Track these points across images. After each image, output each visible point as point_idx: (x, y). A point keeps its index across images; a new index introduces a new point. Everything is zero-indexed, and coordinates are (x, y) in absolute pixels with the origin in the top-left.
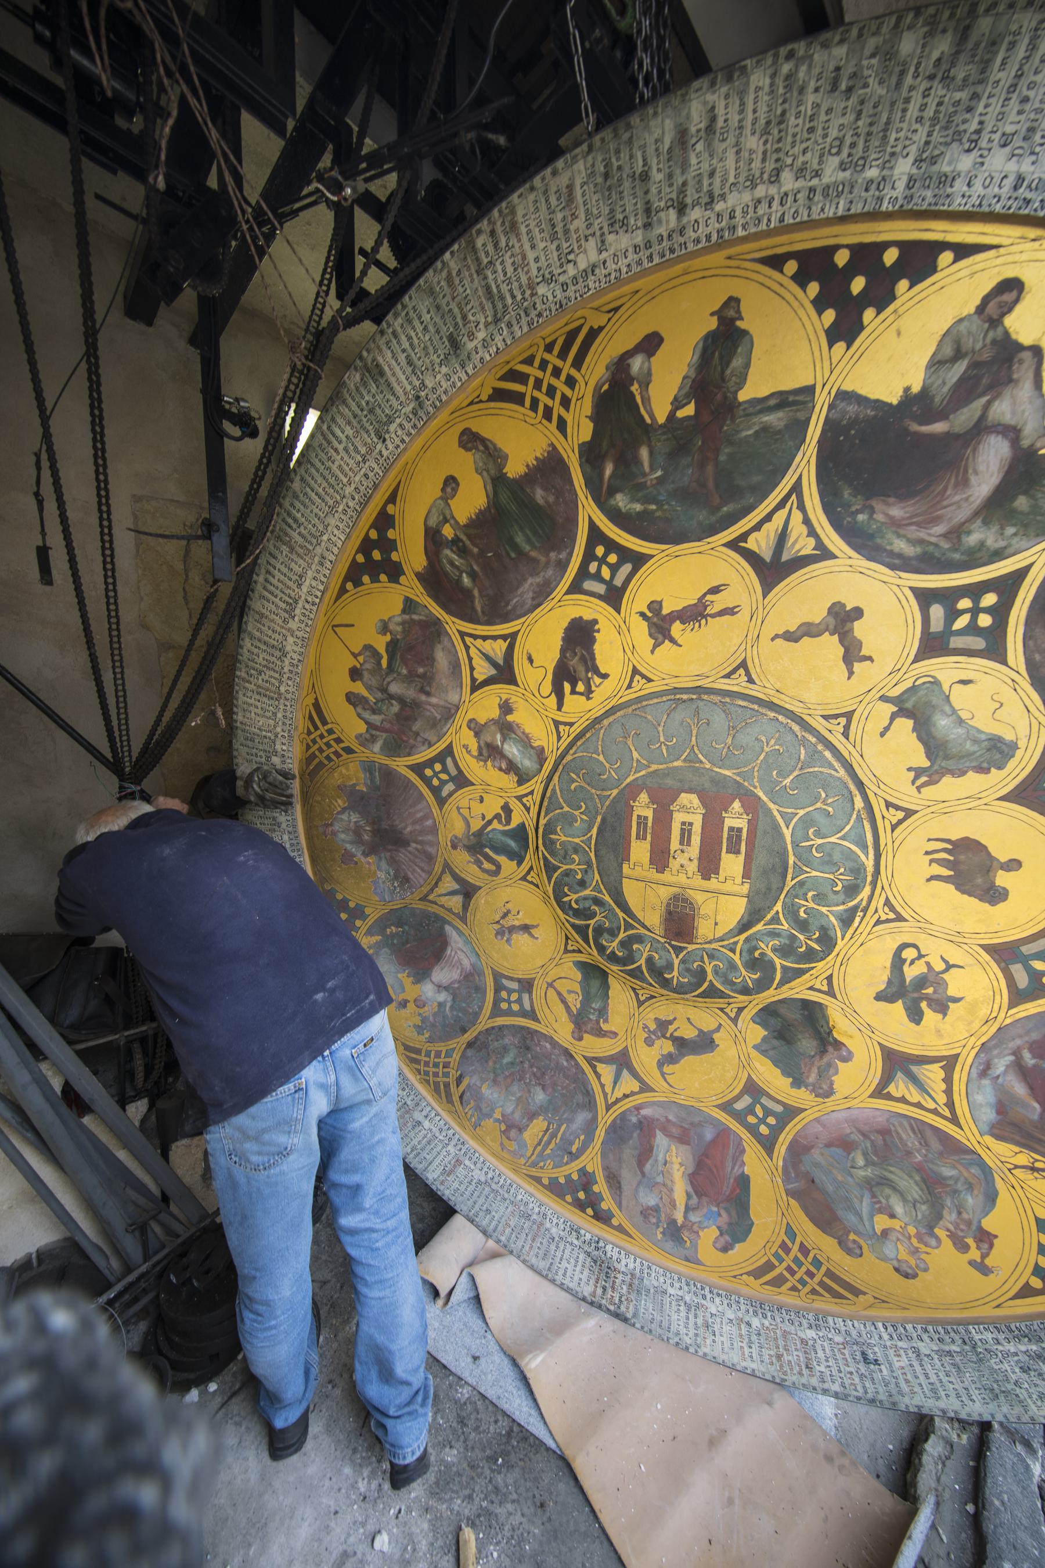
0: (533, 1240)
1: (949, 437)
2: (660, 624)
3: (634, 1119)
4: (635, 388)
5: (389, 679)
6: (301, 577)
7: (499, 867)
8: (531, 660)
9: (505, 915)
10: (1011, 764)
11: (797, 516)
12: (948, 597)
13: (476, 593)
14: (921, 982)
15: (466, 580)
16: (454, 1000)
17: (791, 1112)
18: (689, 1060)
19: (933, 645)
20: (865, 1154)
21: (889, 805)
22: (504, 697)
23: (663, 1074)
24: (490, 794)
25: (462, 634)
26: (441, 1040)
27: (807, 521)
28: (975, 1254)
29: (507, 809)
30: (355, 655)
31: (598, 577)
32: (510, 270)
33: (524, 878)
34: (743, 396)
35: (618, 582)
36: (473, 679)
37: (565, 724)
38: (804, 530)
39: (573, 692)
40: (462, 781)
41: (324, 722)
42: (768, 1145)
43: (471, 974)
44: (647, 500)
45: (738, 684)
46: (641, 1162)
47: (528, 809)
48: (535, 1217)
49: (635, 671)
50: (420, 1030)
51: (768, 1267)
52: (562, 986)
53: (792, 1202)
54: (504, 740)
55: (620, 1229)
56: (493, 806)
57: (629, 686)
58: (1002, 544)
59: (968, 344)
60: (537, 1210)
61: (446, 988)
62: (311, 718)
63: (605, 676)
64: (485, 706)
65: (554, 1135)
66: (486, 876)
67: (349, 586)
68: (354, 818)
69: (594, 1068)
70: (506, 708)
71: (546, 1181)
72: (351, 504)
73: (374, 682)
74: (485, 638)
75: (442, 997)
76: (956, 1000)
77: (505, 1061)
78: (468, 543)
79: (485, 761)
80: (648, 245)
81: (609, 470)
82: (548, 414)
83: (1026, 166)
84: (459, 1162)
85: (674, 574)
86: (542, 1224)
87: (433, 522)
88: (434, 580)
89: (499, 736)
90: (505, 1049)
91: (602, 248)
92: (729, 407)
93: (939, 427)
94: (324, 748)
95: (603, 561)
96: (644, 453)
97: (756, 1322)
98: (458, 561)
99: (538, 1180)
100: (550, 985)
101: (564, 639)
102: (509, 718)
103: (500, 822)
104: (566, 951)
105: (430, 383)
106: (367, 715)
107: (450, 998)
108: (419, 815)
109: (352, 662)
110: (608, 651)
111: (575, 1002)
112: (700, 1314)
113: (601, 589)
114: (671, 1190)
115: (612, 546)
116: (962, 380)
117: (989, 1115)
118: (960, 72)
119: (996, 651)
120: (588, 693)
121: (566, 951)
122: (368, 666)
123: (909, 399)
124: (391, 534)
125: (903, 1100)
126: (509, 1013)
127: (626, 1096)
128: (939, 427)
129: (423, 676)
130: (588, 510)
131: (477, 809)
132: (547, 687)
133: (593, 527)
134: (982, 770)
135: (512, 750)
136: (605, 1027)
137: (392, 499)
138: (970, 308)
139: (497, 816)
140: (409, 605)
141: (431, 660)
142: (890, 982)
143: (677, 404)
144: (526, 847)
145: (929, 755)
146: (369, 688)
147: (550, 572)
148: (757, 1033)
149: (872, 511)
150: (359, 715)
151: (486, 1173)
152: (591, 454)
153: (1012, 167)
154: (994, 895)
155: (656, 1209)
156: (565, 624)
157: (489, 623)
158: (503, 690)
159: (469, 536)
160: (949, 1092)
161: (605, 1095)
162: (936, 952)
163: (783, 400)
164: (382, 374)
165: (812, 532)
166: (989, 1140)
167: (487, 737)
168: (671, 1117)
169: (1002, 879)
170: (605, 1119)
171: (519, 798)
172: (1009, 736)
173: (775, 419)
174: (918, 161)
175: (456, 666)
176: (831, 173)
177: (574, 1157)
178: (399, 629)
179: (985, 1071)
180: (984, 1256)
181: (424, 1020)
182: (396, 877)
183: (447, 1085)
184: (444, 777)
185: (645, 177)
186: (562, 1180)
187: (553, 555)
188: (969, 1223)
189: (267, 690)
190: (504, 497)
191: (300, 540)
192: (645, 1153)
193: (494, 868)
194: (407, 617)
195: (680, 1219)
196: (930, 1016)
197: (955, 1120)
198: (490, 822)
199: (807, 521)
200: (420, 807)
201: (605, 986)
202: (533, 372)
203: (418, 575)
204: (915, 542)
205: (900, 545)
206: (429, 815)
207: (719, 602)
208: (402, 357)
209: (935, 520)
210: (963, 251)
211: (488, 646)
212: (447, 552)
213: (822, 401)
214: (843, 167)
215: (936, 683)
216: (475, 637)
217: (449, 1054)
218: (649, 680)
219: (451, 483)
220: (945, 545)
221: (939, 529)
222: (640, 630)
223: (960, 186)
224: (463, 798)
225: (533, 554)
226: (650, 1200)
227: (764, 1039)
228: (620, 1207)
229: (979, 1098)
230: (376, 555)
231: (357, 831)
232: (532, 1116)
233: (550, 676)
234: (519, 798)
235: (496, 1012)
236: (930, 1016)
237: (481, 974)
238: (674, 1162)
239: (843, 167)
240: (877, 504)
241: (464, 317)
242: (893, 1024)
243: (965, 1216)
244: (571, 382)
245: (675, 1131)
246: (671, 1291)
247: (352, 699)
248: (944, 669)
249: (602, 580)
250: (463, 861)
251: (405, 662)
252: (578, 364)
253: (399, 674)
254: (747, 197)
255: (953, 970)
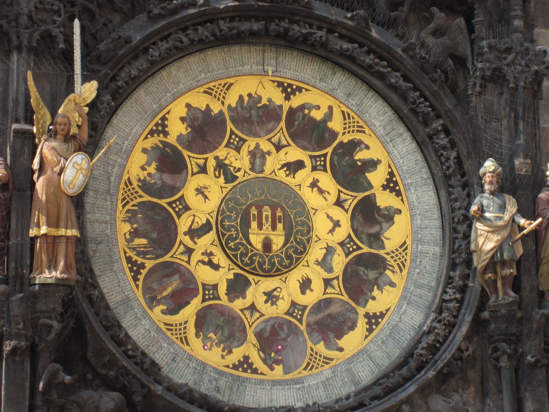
0: (104, 264)
1: (376, 219)
2: (314, 184)
3: (175, 266)
4: (358, 148)
5: (255, 109)
6: (271, 65)
7: (219, 177)
8: (286, 154)
9: (205, 188)
10: (330, 274)
11: (351, 201)
12: (352, 240)
13: (295, 128)
14: (275, 297)
15: (297, 123)
16: (161, 187)
17: (218, 298)
18: (208, 268)
19: (342, 244)
20: (224, 319)
21: (307, 261)
22: (272, 151)
23: (197, 264)
24: (240, 161)
25: (282, 129)
26: (143, 190)
27: (351, 203)
28: (224, 354)
29: (239, 170)
30: (256, 93)
31: (316, 162)
32: (368, 104)
33: (221, 187)
34: (367, 174)
35: (318, 168)
36: (271, 138)
37: (275, 173)
38: (349, 204)
39: (285, 171)
40: (238, 149)
41: (228, 89)
42: (204, 300)
43: (176, 188)
44: (338, 164)
45: (312, 212)
46: (164, 276)
47: (244, 176)
48: (113, 259)
49: (300, 185)
50: (139, 180)
51: (172, 325)
52: (197, 219)
53: (195, 317)
54: (259, 157)
55: (137, 286)
56: (237, 165)
57: (295, 186)
58: (364, 241)
59: (391, 211)
60: (117, 258)
61: (163, 182)
62: (225, 84)
63: (294, 178)
64: (266, 146)
65: (145, 248)
66: (213, 174)
67: (276, 84)
68: (200, 115)
69: (180, 245)
70: (269, 153)
71: (127, 255)
72: (300, 77)
73: (251, 104)
74: (284, 136)
75: (159, 182)
76: (277, 305)
77: (156, 217)
78: (306, 119)
79: (249, 154)
80: (383, 137)
81: (340, 151)
82: (345, 128)
83: (415, 201)
84: (106, 223)
85: (327, 181)
86: (113, 263)
87: (306, 105)
88: (292, 112)
89: (259, 155)
90: (159, 214)
91: (379, 126)
92: (363, 173)
93: (377, 216)
94: (218, 93)
95: (321, 161)
96: (347, 158)
97: (153, 333)
98: (300, 118)
99: (125, 253)
100: (194, 216)
101: (297, 161)
102: (267, 156)
103: (234, 170)
104: (209, 214)
105: (338, 91)
106: (239, 105)
107: (160, 185)
108: (217, 140)
109: (253, 94)
110: (301, 174)
111: (195, 226)
112: (138, 321)
113: (314, 164)
114: (165, 289)
115: (325, 161)
116: (385, 214)
117: (258, 330)
118: (423, 182)
119: (347, 255)
120: (287, 175)
121: (209, 214)
122: (255, 99)
123: (379, 207)
124: (297, 93)
125: (245, 315)
126: (174, 209)
127: (180, 259)
128: (377, 216)
129: (263, 121)
130: (329, 150)
131: (233, 159)
132: (282, 163)
133: (326, 154)
134: (325, 271)
135: (258, 162)
136: (196, 240)
137: (307, 90)
138: (396, 207)
139: (235, 168)
140: (281, 107)
141: (269, 121)
142: (269, 292)
143: (359, 160)
144: (232, 182)
145: (322, 260)
146: (248, 102)
147: (311, 147)
148: (231, 276)
149: (359, 215)
150: (237, 103)
151: (112, 235)
152: (341, 144)
153: (414, 199)
154: (303, 292)
155: (154, 290)
156: (301, 159)
157: (290, 136)
158: (273, 150)
159: (308, 119)
160: (255, 320)
161: (175, 253)
162: (284, 293)
163: (369, 183)
164: (334, 75)
165: (349, 206)
166: (252, 335)
167: (257, 152)
168: (187, 275)
169: (308, 291)
170: (167, 258)
171: (245, 172)
172: (334, 270)
173: (365, 184)
174: (411, 183)
175: (271, 131)
176: (405, 168)
177: (144, 258)
178: (272, 106)
179: (267, 321)
180: (226, 355)
181: (145, 179)
182: (189, 142)
183: (128, 202)
184: (235, 143)
185: (393, 130)
186: (134, 260)
187: (315, 146)
188: (230, 347)
189: (227, 63)
190: (322, 125)
191: (281, 61)
192: (169, 276)
193: (217, 175)
194: (277, 107)
195: (159, 297)
196: (269, 304)
197: (250, 327)
198: (231, 166)
199: (351, 203)
200: (220, 139)
201: (208, 232)
202: (352, 120)
203: (290, 106)
204: (358, 227)
205: (355, 224)
206: (220, 144)
207: (326, 195)
208: (340, 80)
209: (362, 227)
210: (402, 200)
211: (283, 138)
212: (301, 114)
213: (372, 191)
214: (406, 170)
215: (336, 250)
216: (283, 133)
217: (141, 196)
218: (300, 190)
219: (318, 107)
220: (360, 232)
221: (361, 229)
222: (310, 180)
223: (410, 192)
224: (233, 152)
225: (313, 141)
226: (155, 286)
227: (231, 279)
228: (144, 281)
229: (260, 326)
230: (289, 90)
231: (196, 119)
232: (145, 237)
233: (285, 162)
234: (245, 172)
235: (170, 204)
236: (269, 304)
237: (179, 190)
238: (174, 284)
239: (406, 170)
240: (360, 215)
241: (355, 96)
242: (260, 301)
243: (231, 345)
244: (353, 131)
245: (183, 278)
246: (136, 310)
247: (241, 97)
248: (339, 249)
249: (316, 163)
250: (211, 164)
251: (263, 112)
252: (358, 131)
253: (259, 112)
254: (397, 154)
255: (282, 300)
